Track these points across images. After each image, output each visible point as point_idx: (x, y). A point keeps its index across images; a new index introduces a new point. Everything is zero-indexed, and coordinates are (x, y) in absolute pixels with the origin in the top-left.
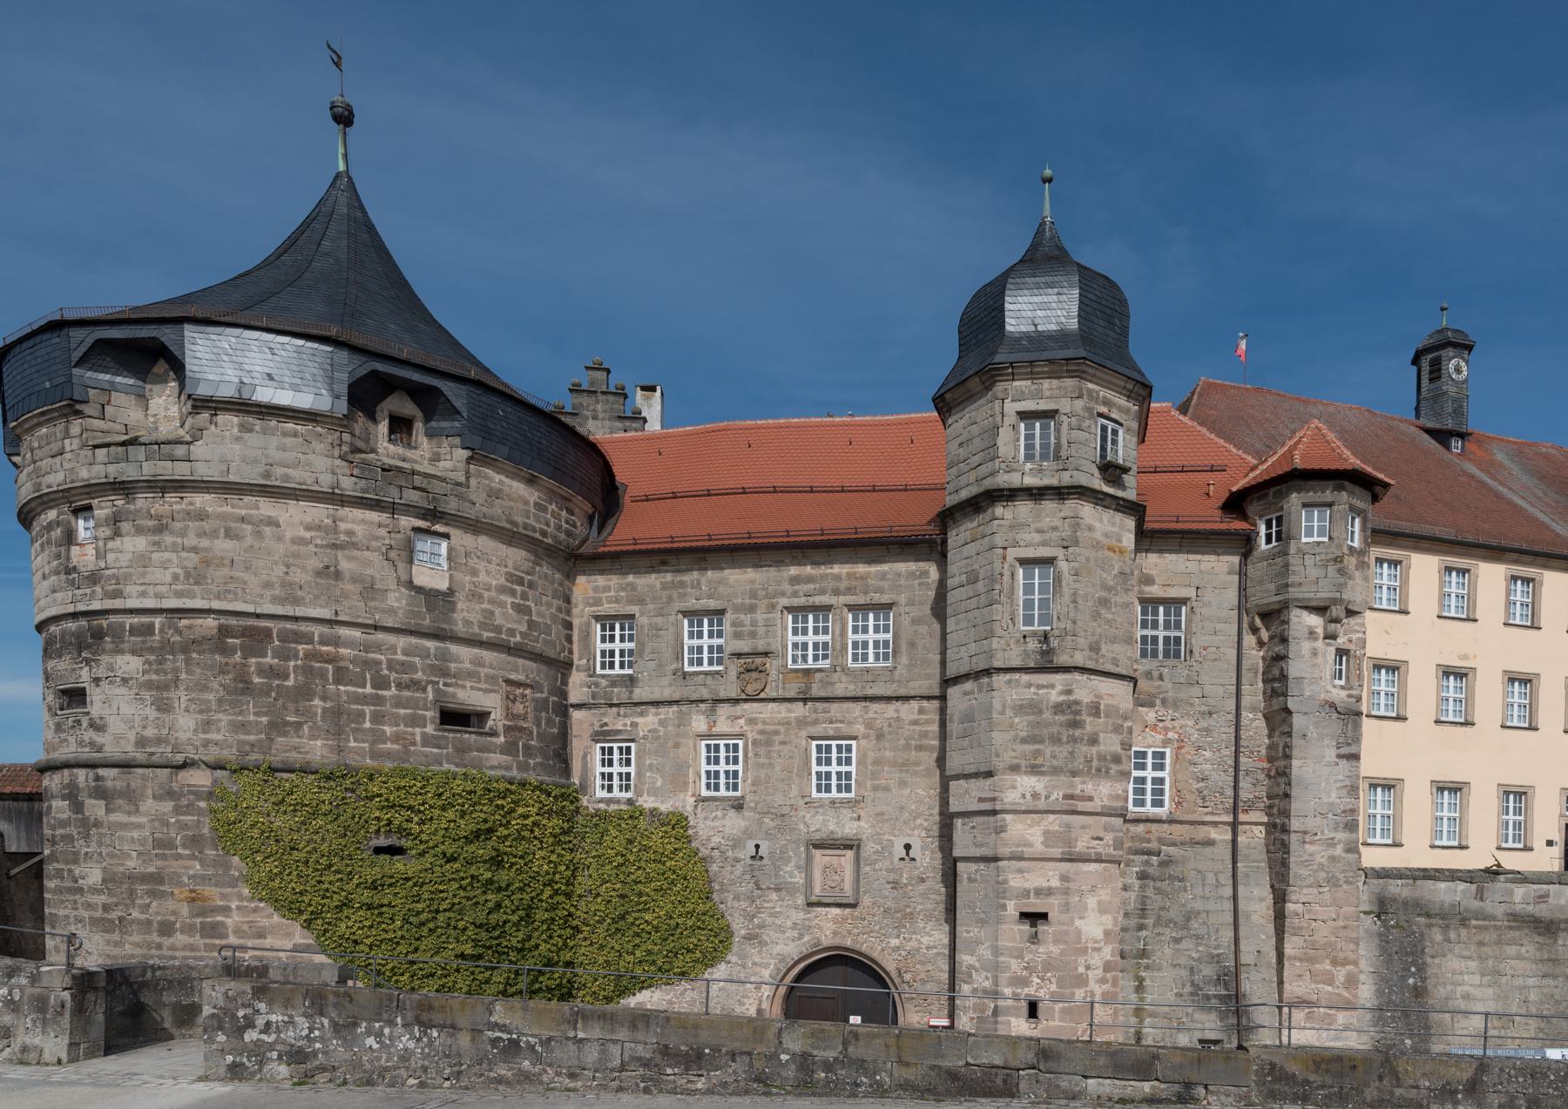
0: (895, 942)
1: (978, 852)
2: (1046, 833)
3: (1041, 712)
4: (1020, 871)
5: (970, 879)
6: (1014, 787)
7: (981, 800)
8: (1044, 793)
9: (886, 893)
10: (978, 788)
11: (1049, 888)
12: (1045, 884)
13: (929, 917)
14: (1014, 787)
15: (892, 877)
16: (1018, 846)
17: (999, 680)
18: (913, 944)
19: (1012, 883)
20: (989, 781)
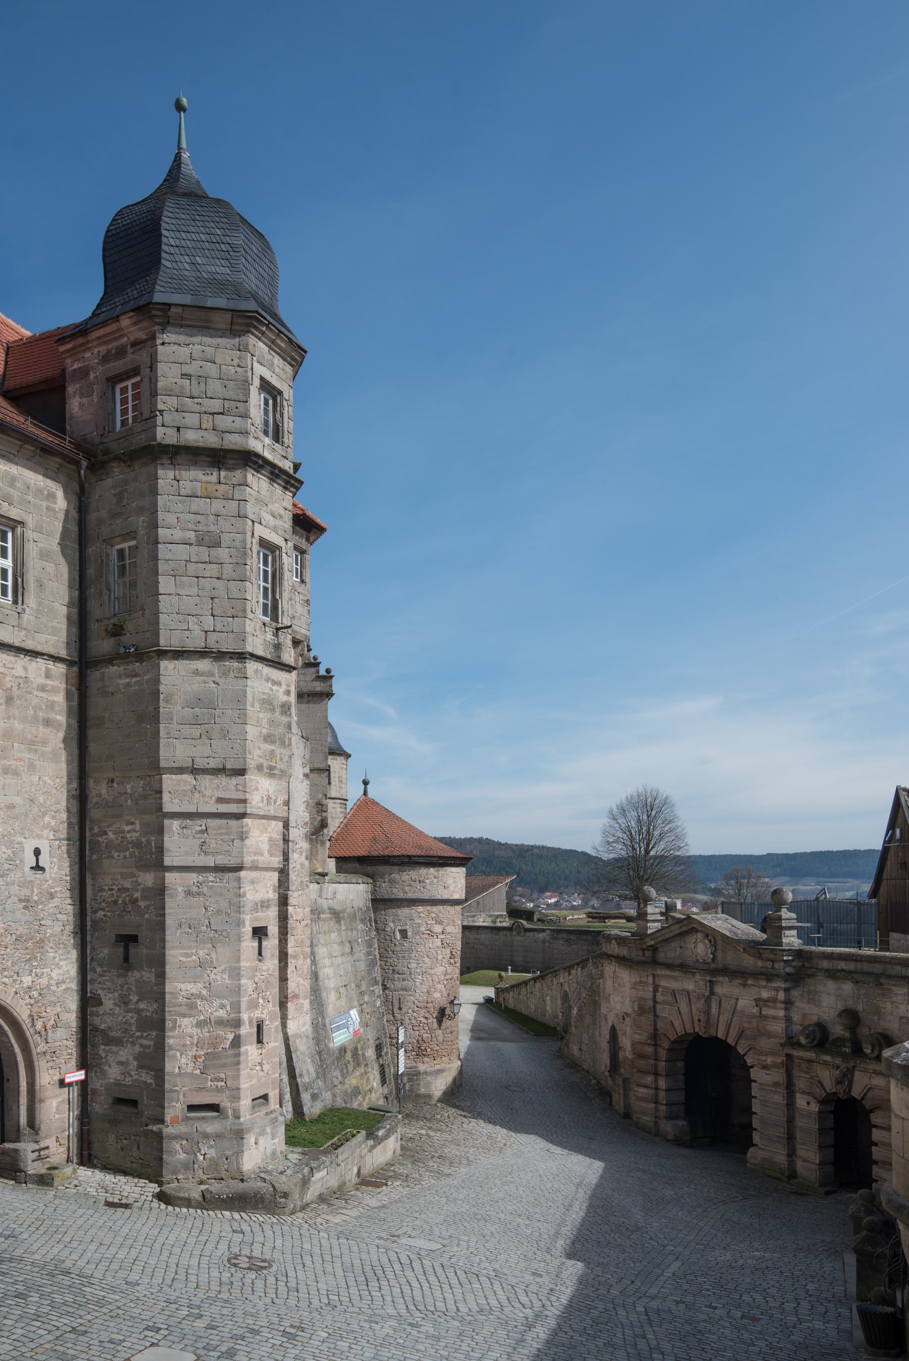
0: (27, 980)
1: (210, 861)
2: (271, 839)
3: (273, 710)
4: (253, 882)
5: (188, 893)
6: (257, 789)
7: (220, 800)
8: (274, 798)
9: (18, 915)
10: (227, 786)
11: (268, 900)
12: (266, 896)
13: (57, 946)
14: (257, 789)
15: (25, 892)
16: (256, 854)
17: (252, 666)
18: (44, 981)
19: (248, 895)
20: (235, 781)
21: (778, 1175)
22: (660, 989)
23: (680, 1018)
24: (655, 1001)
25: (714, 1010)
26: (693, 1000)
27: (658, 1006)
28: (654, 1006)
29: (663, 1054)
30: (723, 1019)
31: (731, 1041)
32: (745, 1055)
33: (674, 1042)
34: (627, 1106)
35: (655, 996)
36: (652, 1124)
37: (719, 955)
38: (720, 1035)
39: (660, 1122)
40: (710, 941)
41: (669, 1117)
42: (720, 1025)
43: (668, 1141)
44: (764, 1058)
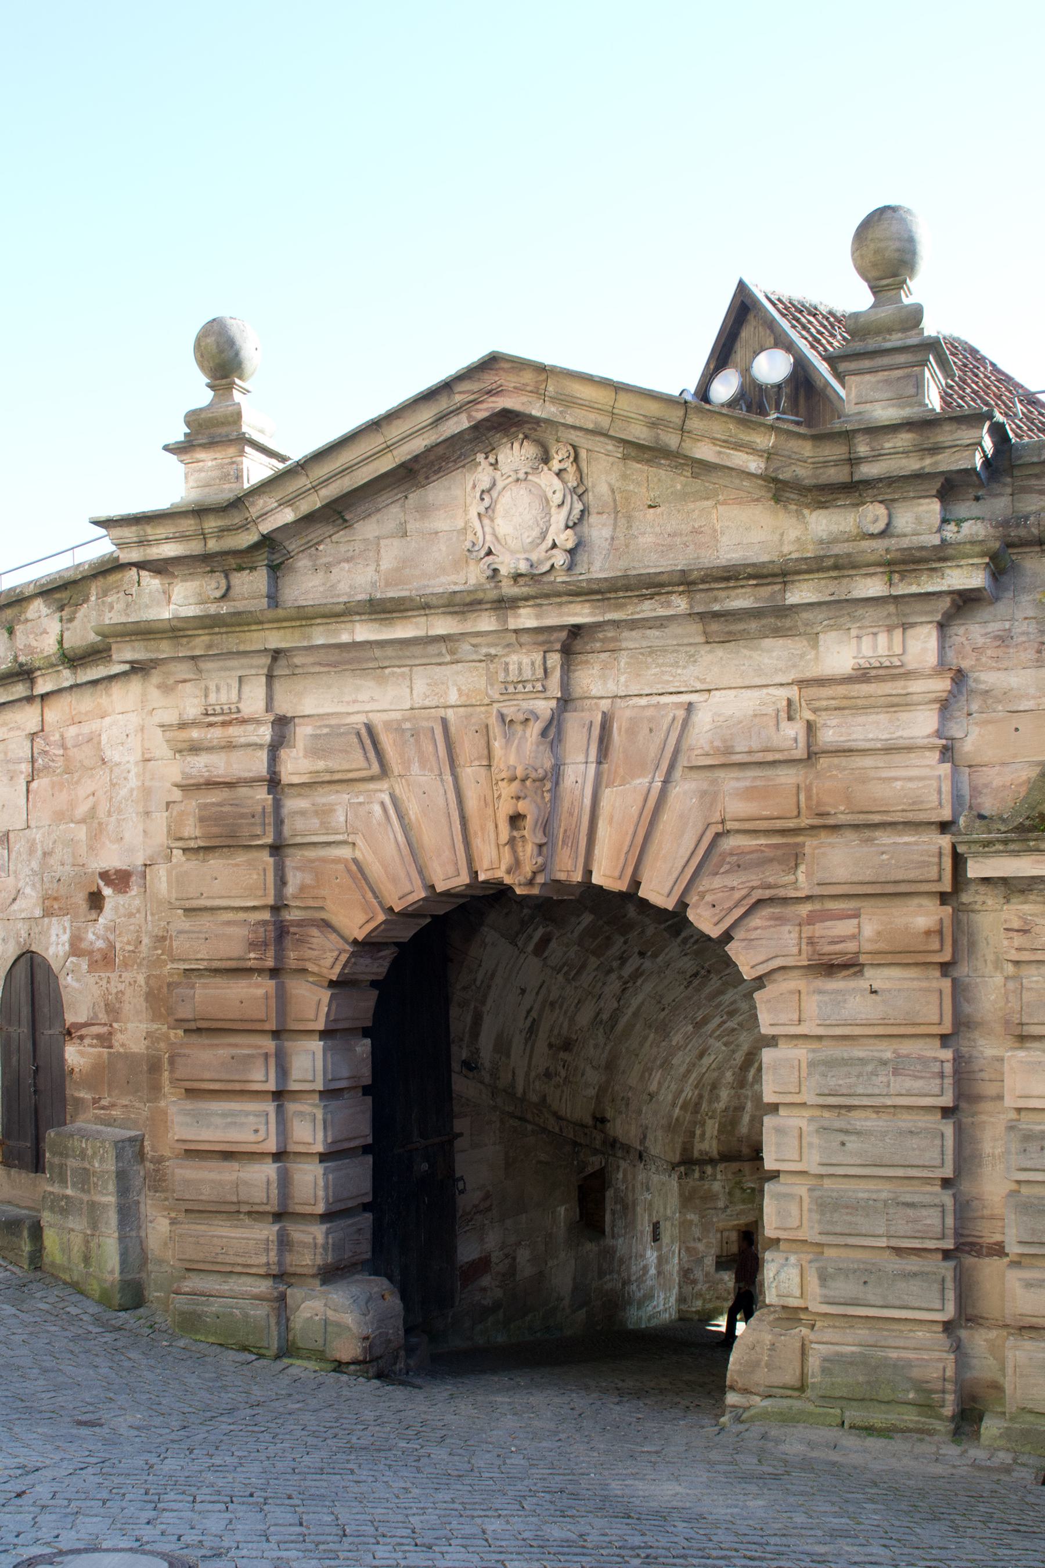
21: (910, 1417)
22: (303, 732)
23: (393, 843)
24: (274, 783)
25: (578, 772)
26: (468, 747)
27: (292, 804)
28: (277, 805)
29: (313, 1003)
30: (622, 805)
31: (658, 891)
32: (727, 937)
33: (365, 947)
34: (133, 1254)
35: (273, 759)
36: (261, 1311)
37: (599, 530)
38: (606, 875)
39: (294, 1294)
40: (559, 474)
41: (331, 1274)
42: (604, 831)
43: (339, 1366)
44: (844, 928)
